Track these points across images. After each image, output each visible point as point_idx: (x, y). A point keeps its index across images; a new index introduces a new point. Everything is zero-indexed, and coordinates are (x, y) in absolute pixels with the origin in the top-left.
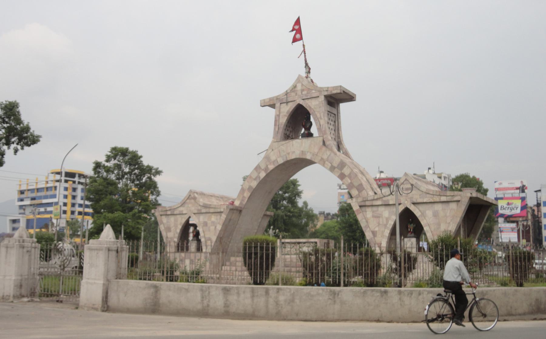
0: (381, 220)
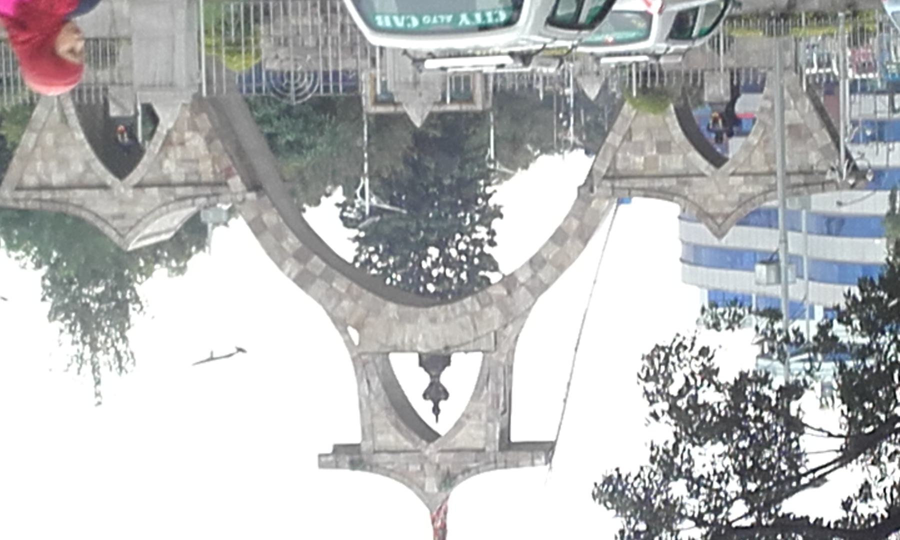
0: (179, 156)
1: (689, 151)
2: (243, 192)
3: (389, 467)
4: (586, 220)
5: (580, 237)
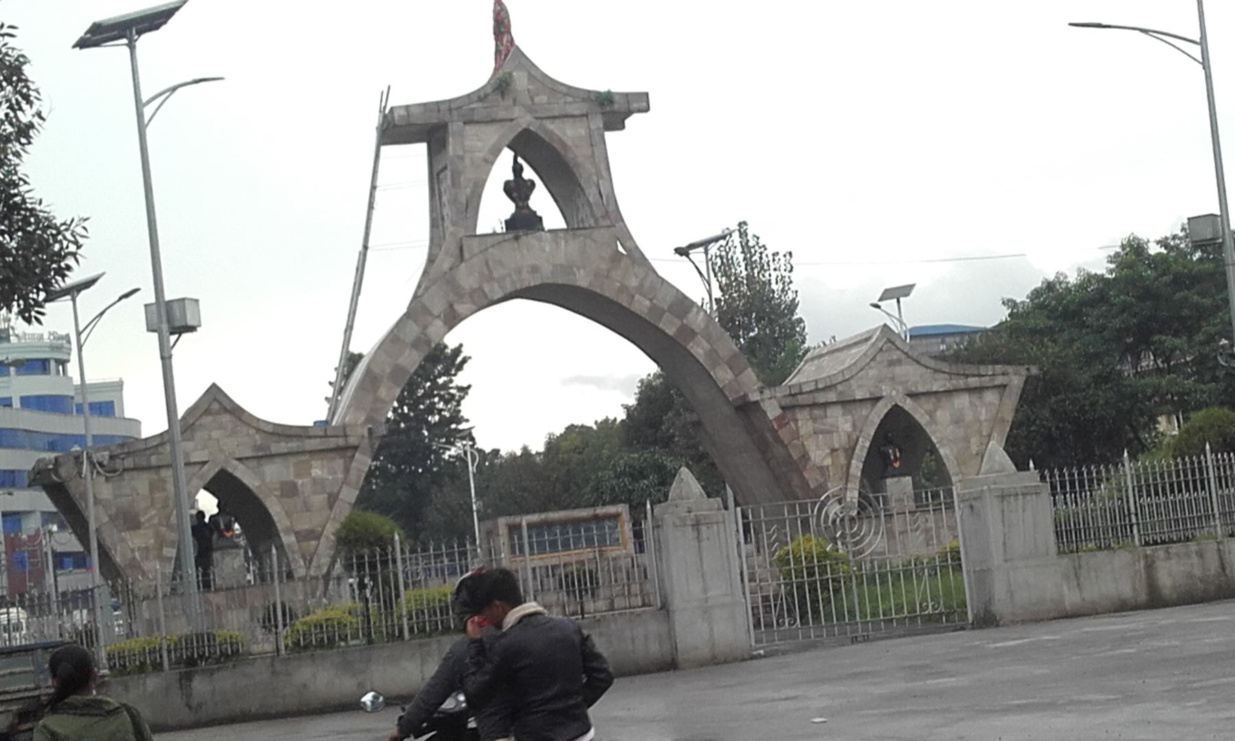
2: (763, 400)
3: (569, 99)
5: (376, 378)
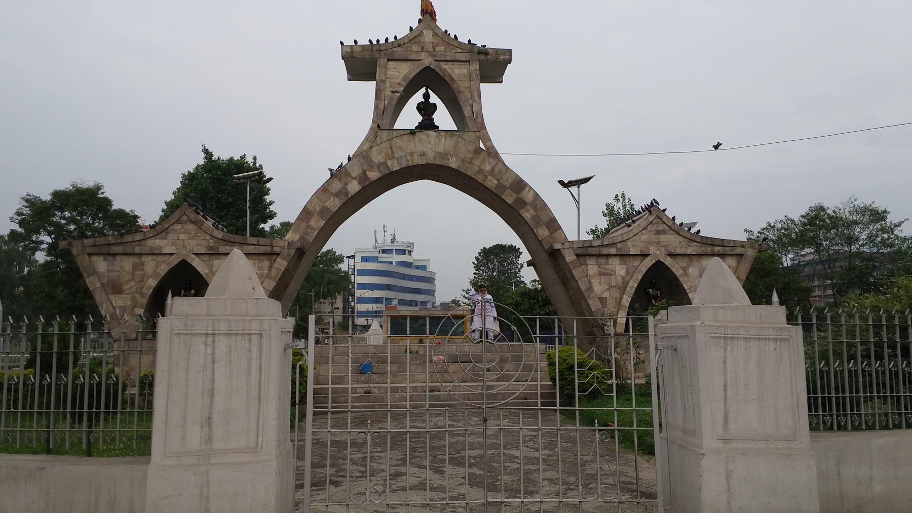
1: (207, 274)
2: (563, 249)
4: (303, 225)
5: (309, 213)
